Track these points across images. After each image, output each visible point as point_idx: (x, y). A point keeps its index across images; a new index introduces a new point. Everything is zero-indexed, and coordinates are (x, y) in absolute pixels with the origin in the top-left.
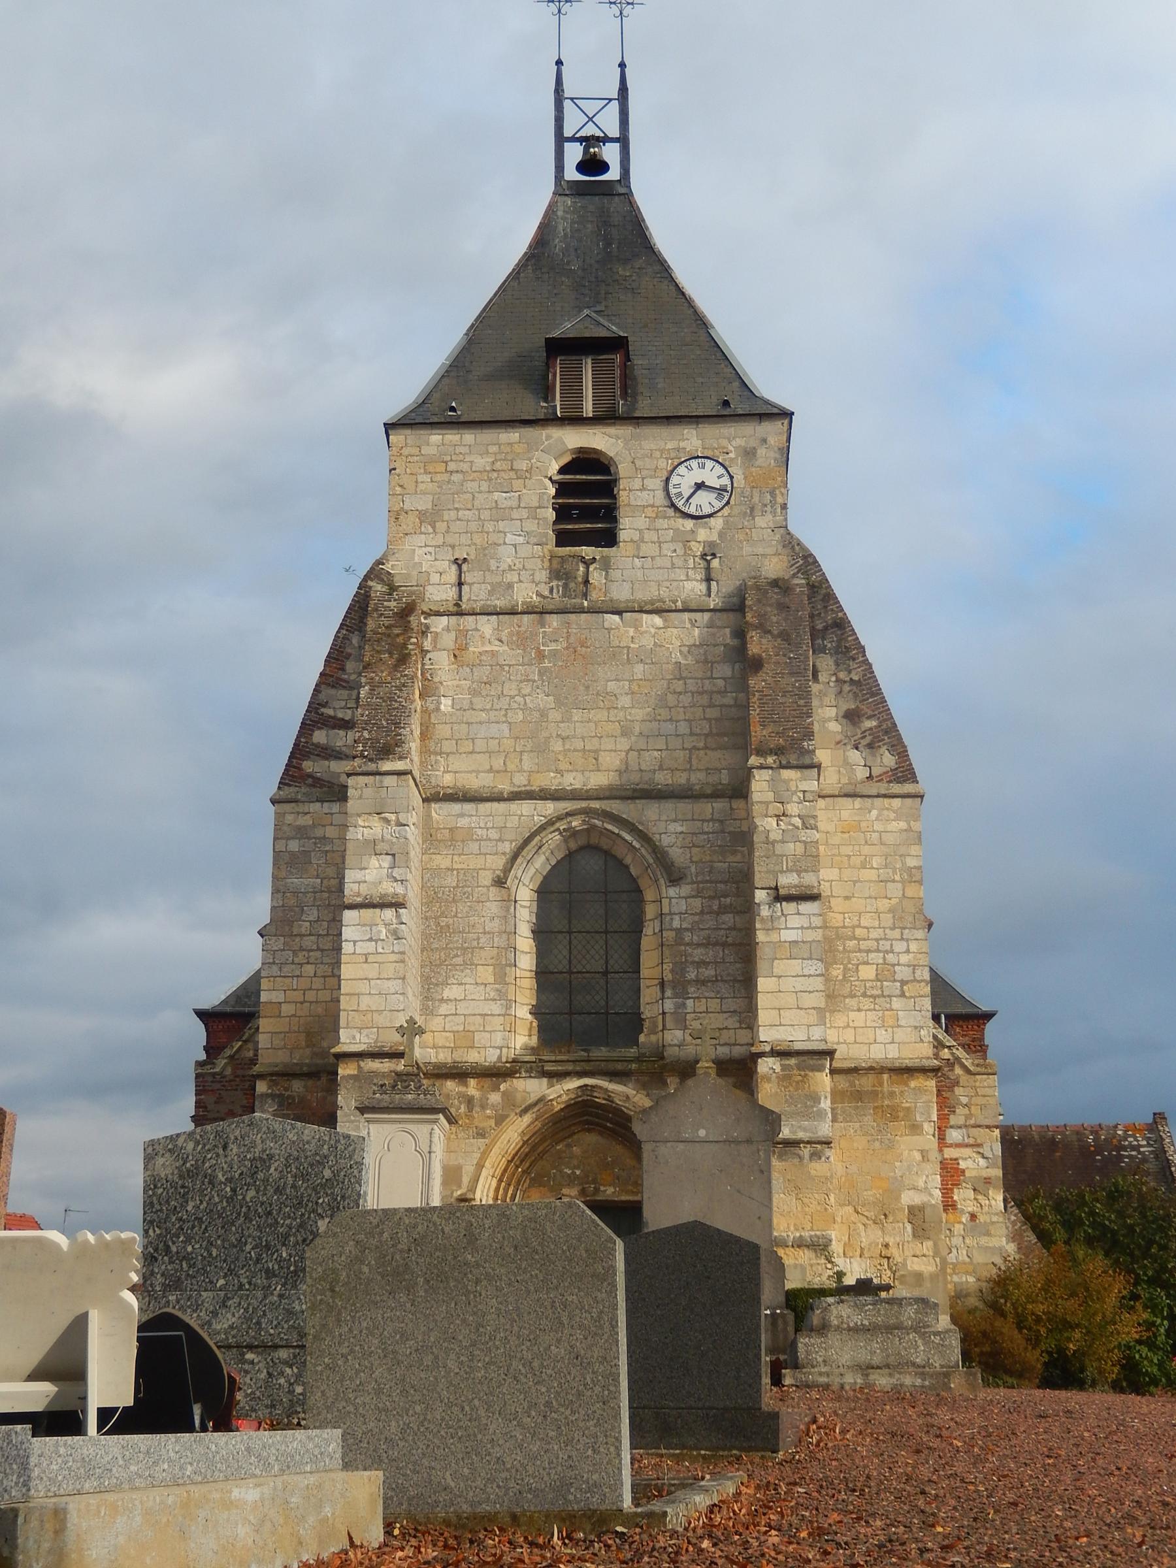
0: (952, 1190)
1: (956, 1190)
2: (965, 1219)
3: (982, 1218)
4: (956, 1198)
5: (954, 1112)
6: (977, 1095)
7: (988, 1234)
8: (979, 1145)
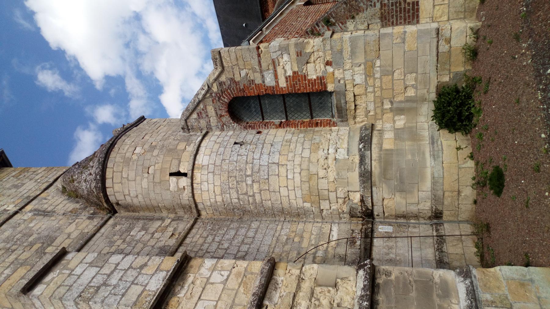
0: (309, 80)
1: (309, 78)
2: (330, 69)
3: (328, 58)
4: (314, 77)
5: (252, 81)
6: (237, 65)
7: (341, 52)
8: (273, 62)
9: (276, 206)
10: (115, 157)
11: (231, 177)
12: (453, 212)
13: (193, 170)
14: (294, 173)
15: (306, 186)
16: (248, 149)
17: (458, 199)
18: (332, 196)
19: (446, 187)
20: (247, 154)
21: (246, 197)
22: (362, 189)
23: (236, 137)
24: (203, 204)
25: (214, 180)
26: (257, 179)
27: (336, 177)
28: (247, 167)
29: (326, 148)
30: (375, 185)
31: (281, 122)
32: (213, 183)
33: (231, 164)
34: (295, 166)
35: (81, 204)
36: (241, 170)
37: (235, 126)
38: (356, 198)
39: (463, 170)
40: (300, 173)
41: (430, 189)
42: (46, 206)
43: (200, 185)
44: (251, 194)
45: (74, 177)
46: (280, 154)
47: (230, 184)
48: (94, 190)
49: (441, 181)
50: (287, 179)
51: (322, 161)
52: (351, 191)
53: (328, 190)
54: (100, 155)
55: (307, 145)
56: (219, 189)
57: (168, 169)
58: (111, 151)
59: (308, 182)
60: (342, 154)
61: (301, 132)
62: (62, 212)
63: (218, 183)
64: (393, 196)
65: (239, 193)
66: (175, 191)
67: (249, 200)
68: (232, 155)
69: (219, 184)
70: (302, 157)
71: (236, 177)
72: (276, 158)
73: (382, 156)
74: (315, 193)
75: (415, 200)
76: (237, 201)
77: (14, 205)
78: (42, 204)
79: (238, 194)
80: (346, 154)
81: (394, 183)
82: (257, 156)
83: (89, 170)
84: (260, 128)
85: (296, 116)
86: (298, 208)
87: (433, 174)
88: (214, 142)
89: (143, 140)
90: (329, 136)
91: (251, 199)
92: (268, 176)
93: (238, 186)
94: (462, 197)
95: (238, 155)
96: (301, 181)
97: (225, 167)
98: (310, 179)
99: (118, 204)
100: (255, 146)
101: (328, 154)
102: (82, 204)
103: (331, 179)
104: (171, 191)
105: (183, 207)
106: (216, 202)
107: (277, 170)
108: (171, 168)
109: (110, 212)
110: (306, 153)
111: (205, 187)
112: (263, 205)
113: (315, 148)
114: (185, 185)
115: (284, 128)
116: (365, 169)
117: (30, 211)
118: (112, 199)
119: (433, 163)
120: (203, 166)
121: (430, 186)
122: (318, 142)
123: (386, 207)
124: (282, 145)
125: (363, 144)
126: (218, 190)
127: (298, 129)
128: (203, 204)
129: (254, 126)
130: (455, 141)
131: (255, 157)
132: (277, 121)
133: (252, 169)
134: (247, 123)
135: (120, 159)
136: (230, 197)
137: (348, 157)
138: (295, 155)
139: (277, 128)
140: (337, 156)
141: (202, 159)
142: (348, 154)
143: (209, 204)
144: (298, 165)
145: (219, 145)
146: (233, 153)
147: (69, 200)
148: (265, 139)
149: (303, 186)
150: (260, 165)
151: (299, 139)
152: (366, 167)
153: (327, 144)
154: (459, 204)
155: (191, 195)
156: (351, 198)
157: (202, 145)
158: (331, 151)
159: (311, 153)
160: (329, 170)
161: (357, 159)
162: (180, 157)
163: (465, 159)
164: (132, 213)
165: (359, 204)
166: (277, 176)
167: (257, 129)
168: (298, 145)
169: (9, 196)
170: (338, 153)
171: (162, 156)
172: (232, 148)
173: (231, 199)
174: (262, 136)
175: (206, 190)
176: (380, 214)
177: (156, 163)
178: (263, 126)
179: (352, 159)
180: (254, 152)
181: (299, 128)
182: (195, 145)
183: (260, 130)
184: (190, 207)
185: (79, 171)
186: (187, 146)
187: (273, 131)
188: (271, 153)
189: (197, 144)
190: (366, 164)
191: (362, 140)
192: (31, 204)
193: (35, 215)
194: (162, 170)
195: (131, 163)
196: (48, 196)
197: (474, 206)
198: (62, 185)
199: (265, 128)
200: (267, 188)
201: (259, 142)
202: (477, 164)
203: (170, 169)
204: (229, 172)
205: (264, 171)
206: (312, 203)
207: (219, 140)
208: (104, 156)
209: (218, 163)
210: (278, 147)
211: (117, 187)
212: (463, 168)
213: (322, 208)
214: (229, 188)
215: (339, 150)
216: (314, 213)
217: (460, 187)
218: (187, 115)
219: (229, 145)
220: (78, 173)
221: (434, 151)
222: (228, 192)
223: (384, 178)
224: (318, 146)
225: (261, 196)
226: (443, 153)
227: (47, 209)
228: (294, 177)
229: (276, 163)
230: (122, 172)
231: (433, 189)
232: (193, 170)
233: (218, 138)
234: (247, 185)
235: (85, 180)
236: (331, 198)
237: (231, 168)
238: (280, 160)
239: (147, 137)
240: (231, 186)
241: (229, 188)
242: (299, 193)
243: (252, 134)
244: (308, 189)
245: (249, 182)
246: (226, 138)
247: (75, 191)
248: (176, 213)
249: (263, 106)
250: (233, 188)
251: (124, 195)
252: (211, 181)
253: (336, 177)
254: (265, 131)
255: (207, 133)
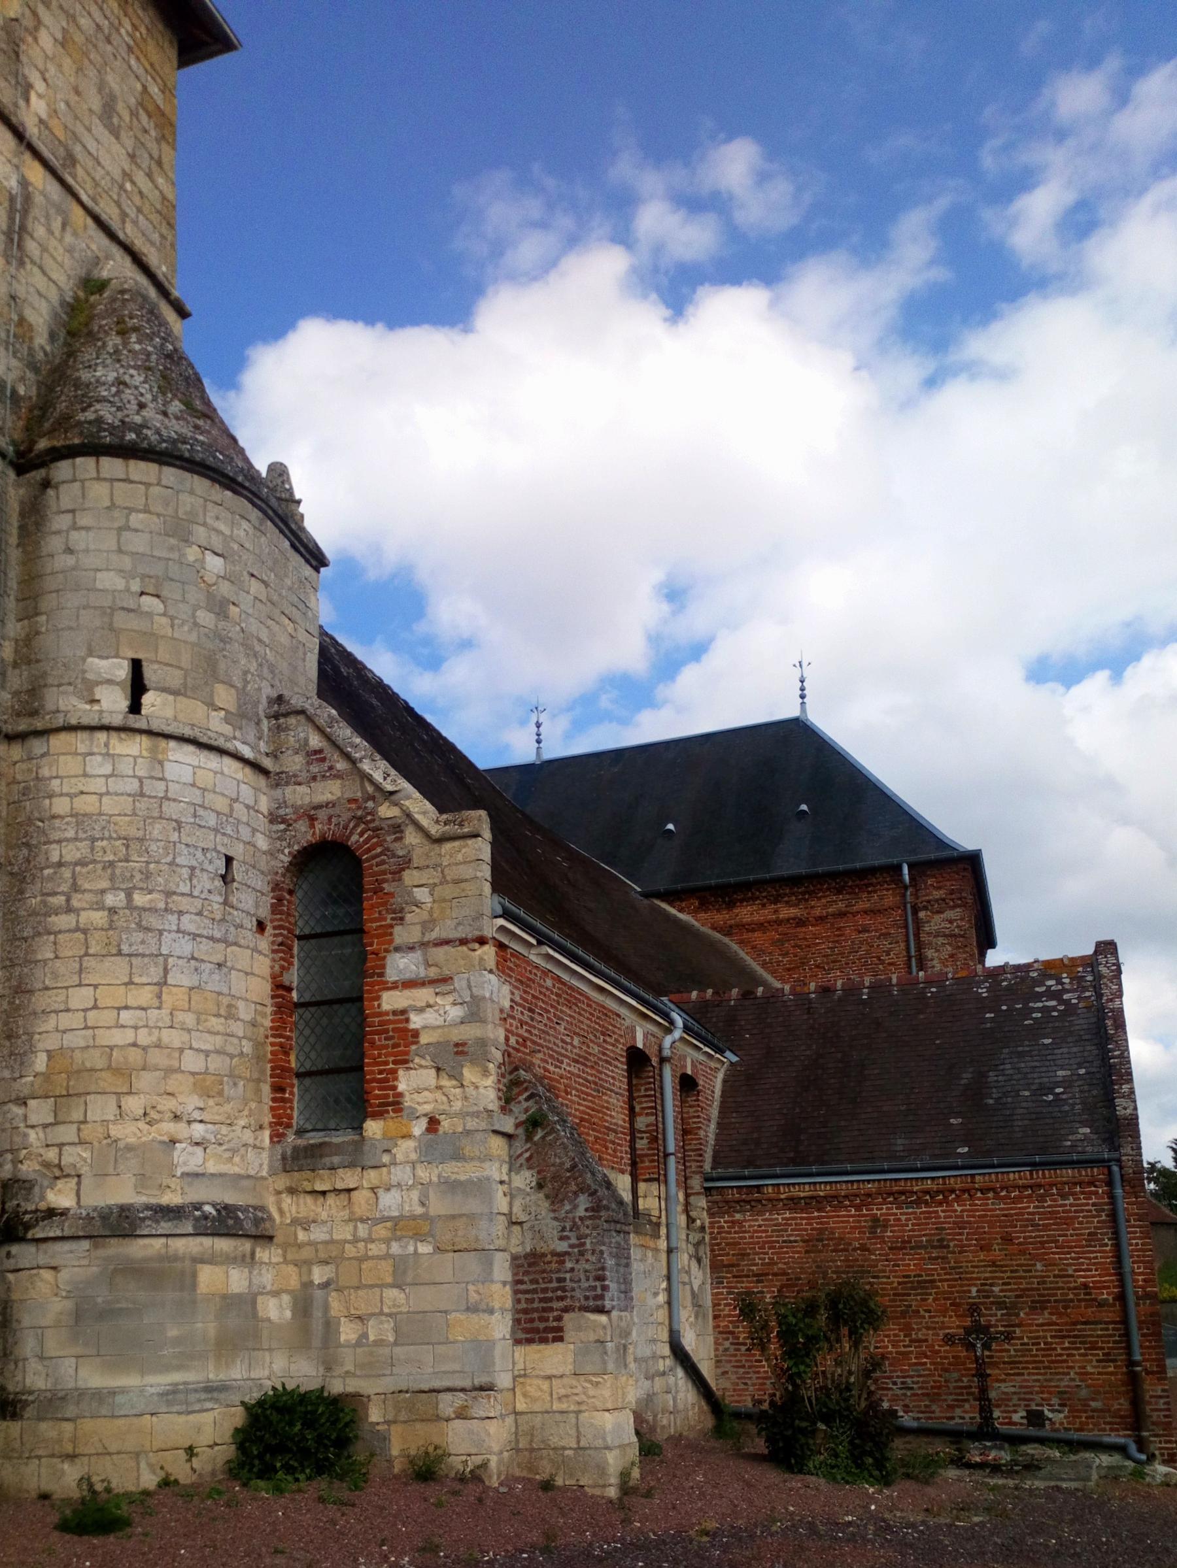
0: (394, 1072)
1: (401, 1073)
3: (445, 1125)
4: (402, 1087)
7: (458, 1156)
9: (38, 972)
10: (192, 492)
11: (127, 847)
12: (17, 1445)
13: (149, 733)
14: (136, 1028)
15: (96, 1059)
16: (211, 897)
17: (53, 1456)
18: (67, 1133)
19: (87, 1425)
20: (196, 893)
21: (64, 888)
22: (84, 1213)
23: (249, 859)
24: (43, 755)
25: (117, 794)
26: (121, 923)
27: (121, 1144)
28: (154, 896)
29: (205, 1116)
30: (96, 1247)
31: (289, 989)
32: (108, 793)
33: (165, 848)
34: (156, 1032)
35: (48, 348)
36: (148, 876)
37: (282, 857)
38: (61, 1197)
39: (133, 1464)
40: (135, 1045)
41: (81, 1384)
42: (40, 231)
43: (104, 751)
44: (75, 903)
45: (134, 338)
46: (191, 989)
47: (105, 843)
48: (90, 415)
49: (104, 1412)
50: (119, 1009)
51: (168, 1104)
52: (79, 1184)
53: (85, 1122)
54: (203, 443)
55: (217, 1064)
56: (89, 809)
57: (151, 656)
58: (213, 480)
59: (109, 1068)
60: (188, 1159)
61: (258, 1045)
62: (21, 291)
63: (108, 805)
64: (64, 1294)
65: (78, 869)
66: (84, 672)
67: (55, 894)
68: (192, 850)
69: (106, 809)
70: (181, 1050)
71: (127, 861)
72: (180, 978)
73: (178, 1265)
74: (76, 1085)
75: (52, 1349)
76: (55, 858)
77: (44, 116)
78: (47, 217)
79: (76, 864)
80: (186, 1169)
81: (102, 1296)
82: (188, 923)
83: (154, 399)
84: (275, 928)
85: (307, 1032)
86: (31, 1035)
87: (123, 1390)
88: (234, 796)
89: (246, 577)
90: (242, 1123)
91: (60, 900)
92: (130, 955)
93: (99, 866)
94: (59, 1466)
95: (193, 868)
96: (111, 1048)
97: (157, 830)
98: (117, 1071)
99: (46, 484)
100: (218, 917)
101: (189, 1122)
102: (46, 354)
103: (115, 1131)
104: (84, 660)
105: (35, 691)
106: (50, 797)
107: (144, 980)
108: (156, 666)
109: (20, 454)
110: (192, 1062)
111: (99, 766)
112: (39, 934)
113: (207, 1086)
114: (105, 705)
115: (273, 997)
116: (143, 1220)
117: (24, 183)
118: (62, 470)
119: (153, 1390)
120: (161, 763)
121: (89, 1385)
122: (226, 1093)
123: (31, 1276)
124: (219, 994)
125: (214, 1213)
126: (86, 804)
127: (267, 1037)
128: (43, 755)
129: (281, 913)
130: (211, 1443)
131: (185, 919)
132: (293, 977)
133: (149, 909)
134: (291, 892)
135: (188, 508)
136: (67, 840)
137: (179, 1174)
138: (189, 1031)
139: (274, 977)
140: (184, 1145)
141: (182, 764)
142: (188, 1174)
143: (45, 772)
144: (159, 1040)
145: (226, 810)
146: (199, 854)
147: (61, 305)
148: (240, 946)
149: (96, 1053)
150: (161, 932)
151: (235, 1041)
152: (148, 1222)
153: (217, 1118)
154: (39, 1457)
155: (74, 722)
156: (60, 1184)
157: (227, 760)
158: (198, 1130)
159: (193, 1074)
160: (141, 1125)
161: (171, 1198)
162: (189, 693)
163: (162, 1468)
164: (16, 524)
165: (43, 1206)
166: (126, 980)
167: (272, 921)
168: (219, 1038)
169: (77, 92)
170: (190, 1149)
171: (193, 638)
172: (215, 849)
173: (59, 842)
174: (248, 936)
175: (88, 769)
176: (12, 1261)
177: (172, 618)
178: (280, 939)
179: (173, 1186)
180: (200, 914)
181: (271, 1040)
182: (228, 739)
183: (269, 930)
184: (34, 713)
185: (154, 357)
186: (223, 713)
187: (263, 965)
188: (198, 964)
189: (229, 746)
190: (157, 1222)
191: (227, 1211)
192: (49, 177)
193: (12, 199)
194: (151, 638)
195: (173, 541)
196: (75, 234)
197: (34, 1494)
198: (109, 280)
199: (273, 943)
200: (91, 951)
201: (232, 929)
202: (146, 1493)
203: (152, 662)
204: (141, 840)
205: (143, 942)
206: (47, 1076)
207: (240, 811)
208: (199, 457)
209: (170, 809)
210: (215, 982)
211: (99, 492)
212: (138, 1464)
213: (32, 1103)
214: (93, 840)
215: (199, 1150)
216: (15, 1080)
217: (86, 1459)
218: (316, 719)
219: (226, 840)
220: (149, 354)
221: (187, 1391)
222: (81, 835)
223: (115, 1271)
224: (212, 1094)
225: (69, 931)
226: (179, 1413)
227: (32, 237)
228: (123, 1026)
229: (165, 977)
230: (146, 511)
231: (82, 1394)
232: (149, 733)
233: (248, 807)
234: (103, 892)
235: (125, 384)
236: (61, 1128)
237: (153, 847)
238: (174, 990)
239: (255, 587)
240: (99, 844)
241: (93, 840)
242: (76, 1040)
243: (257, 906)
244: (88, 1065)
245: (110, 900)
246: (245, 832)
247: (90, 333)
248: (15, 665)
249: (336, 940)
250: (92, 849)
251: (73, 511)
252: (115, 785)
253: (121, 1144)
254: (264, 943)
255: (264, 772)
